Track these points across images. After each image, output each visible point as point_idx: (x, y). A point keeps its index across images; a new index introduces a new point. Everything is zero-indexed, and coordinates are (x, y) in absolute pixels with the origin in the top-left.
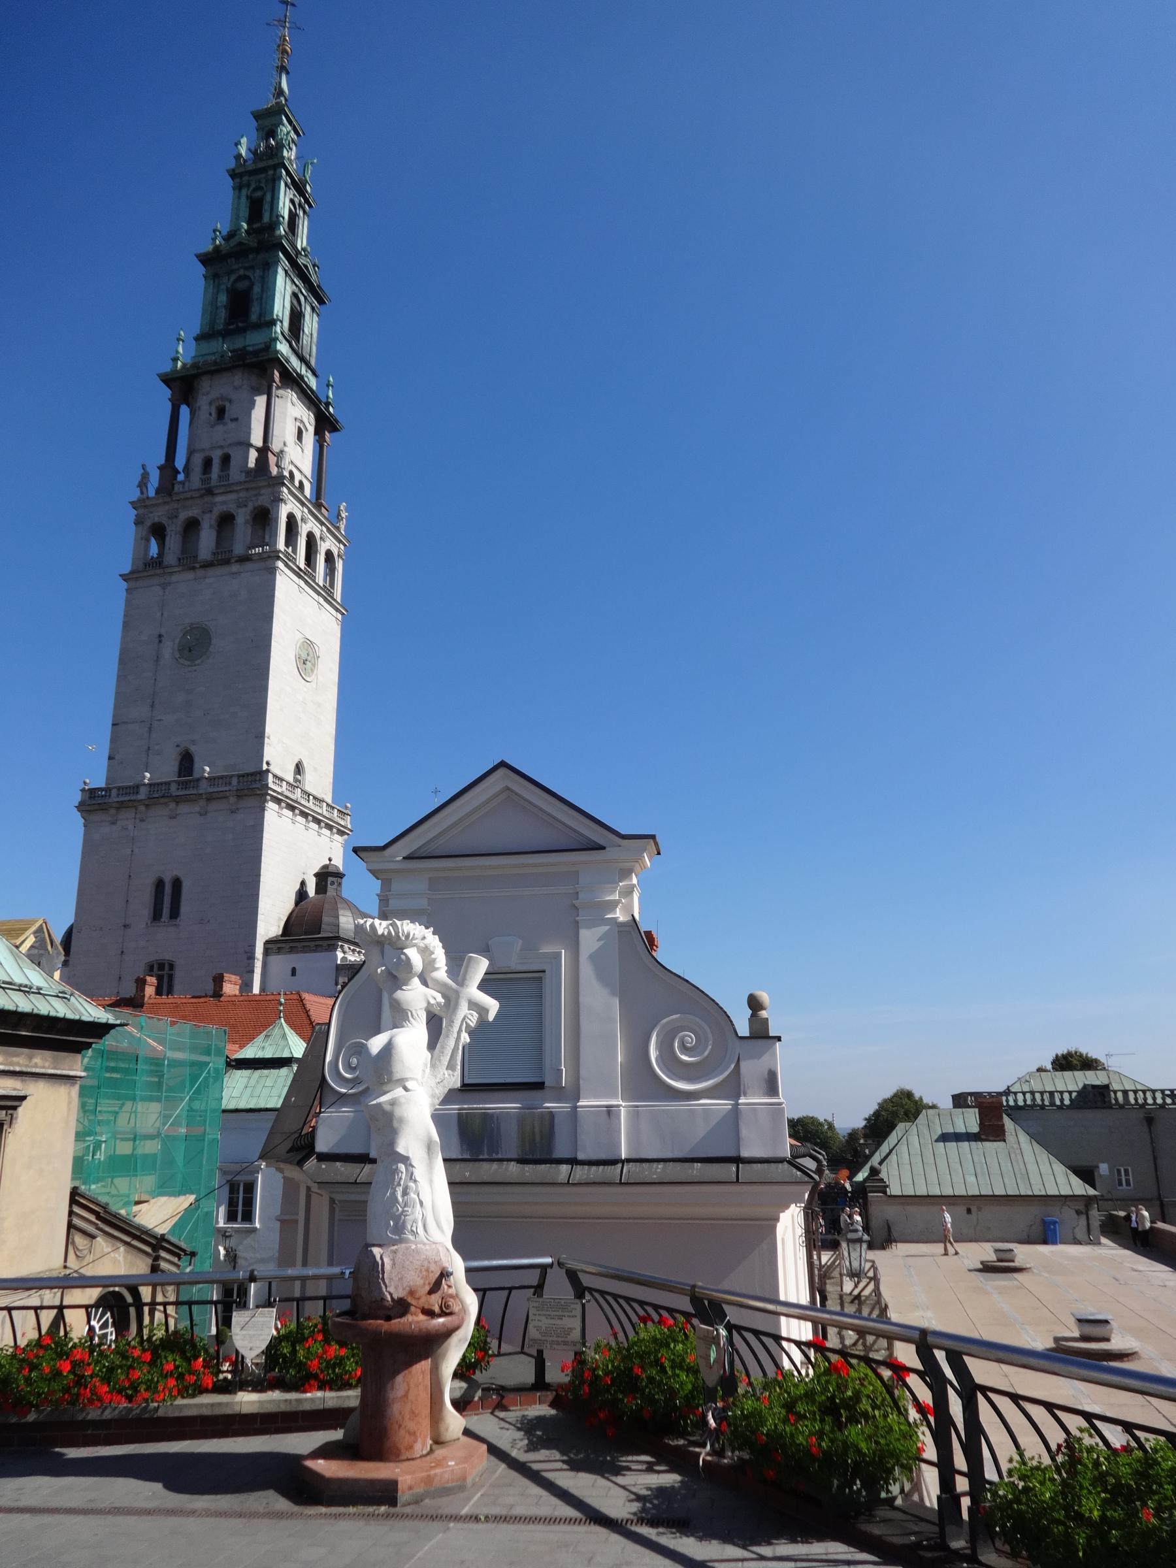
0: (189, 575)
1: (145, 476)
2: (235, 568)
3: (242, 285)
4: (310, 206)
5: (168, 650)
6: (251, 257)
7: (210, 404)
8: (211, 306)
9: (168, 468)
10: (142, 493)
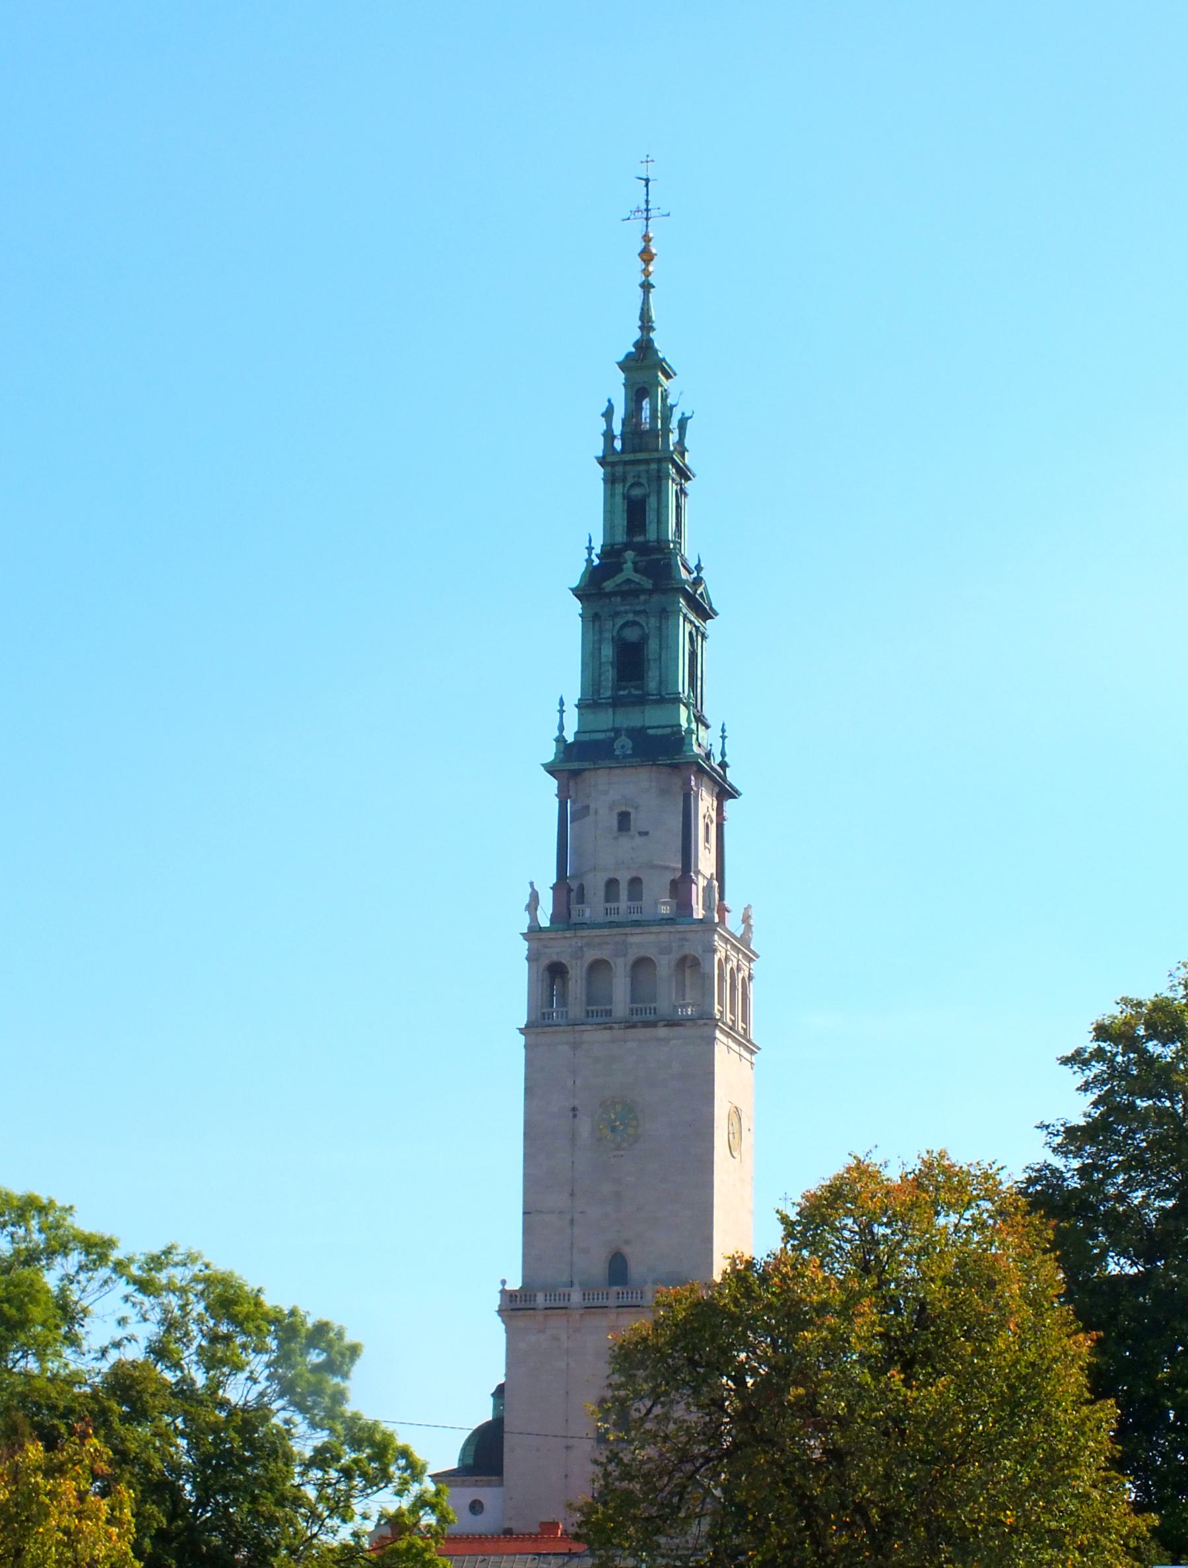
0: (606, 1035)
1: (534, 898)
2: (662, 1032)
3: (632, 635)
5: (585, 1128)
6: (642, 598)
7: (611, 809)
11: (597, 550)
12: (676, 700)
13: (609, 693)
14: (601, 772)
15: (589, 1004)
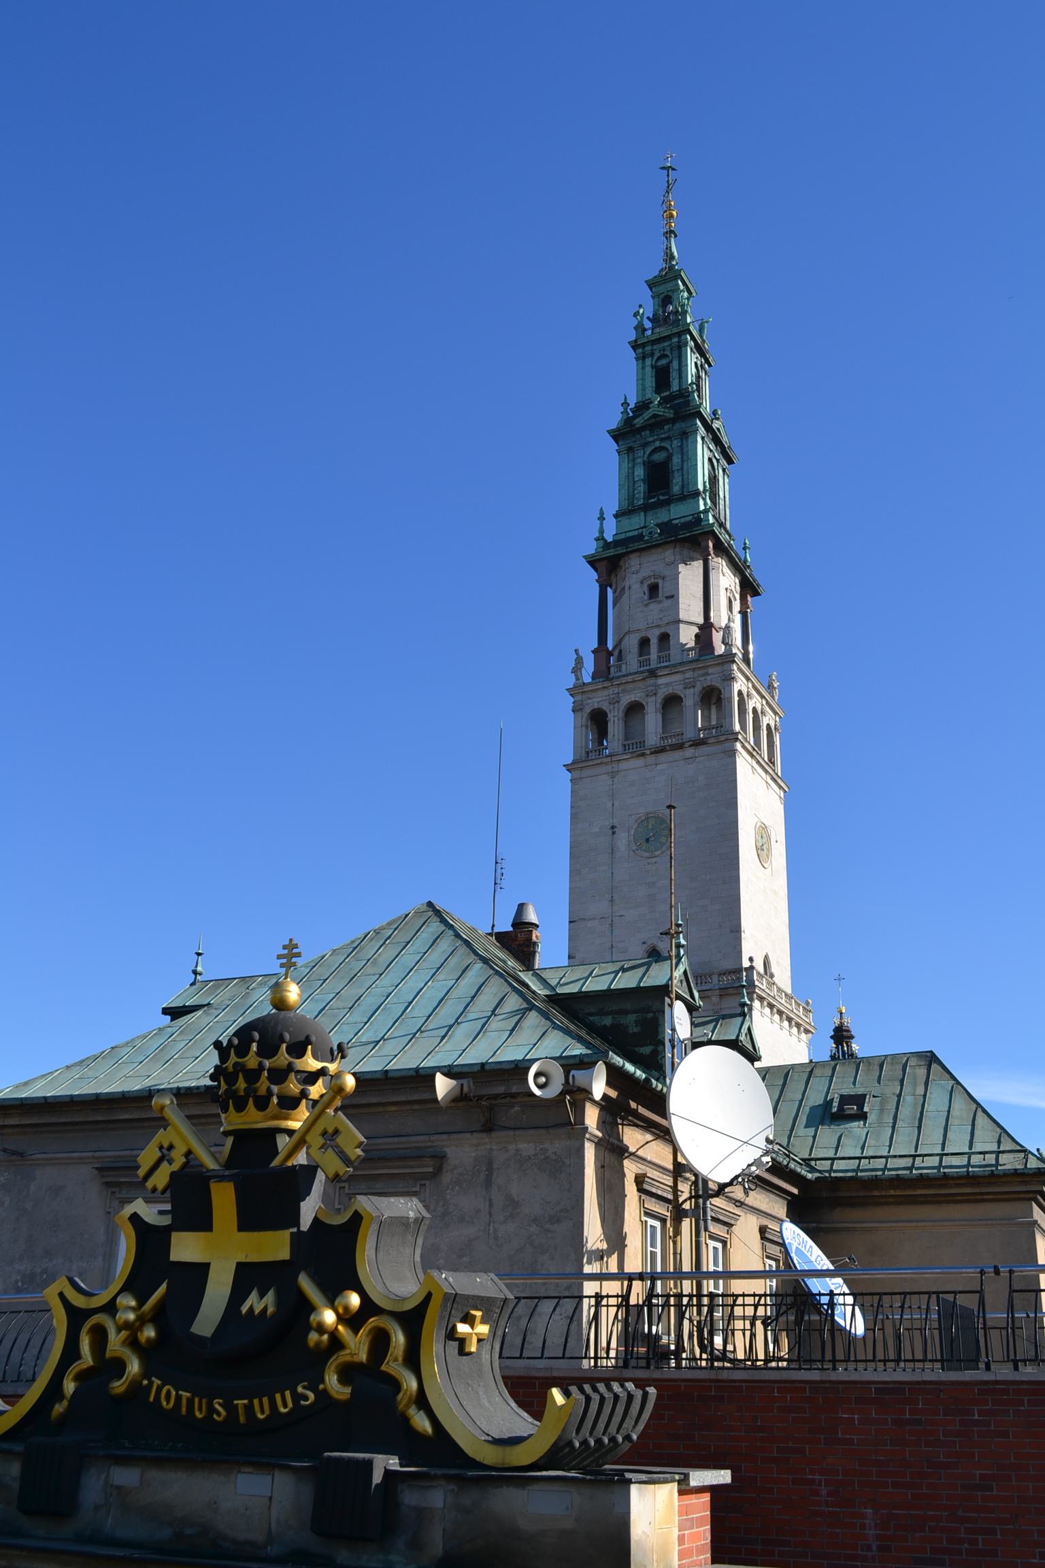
0: (640, 762)
2: (689, 752)
3: (660, 457)
4: (710, 365)
5: (623, 840)
7: (642, 583)
8: (628, 481)
9: (601, 651)
10: (577, 679)
11: (632, 406)
12: (696, 494)
13: (641, 502)
14: (632, 556)
15: (626, 739)
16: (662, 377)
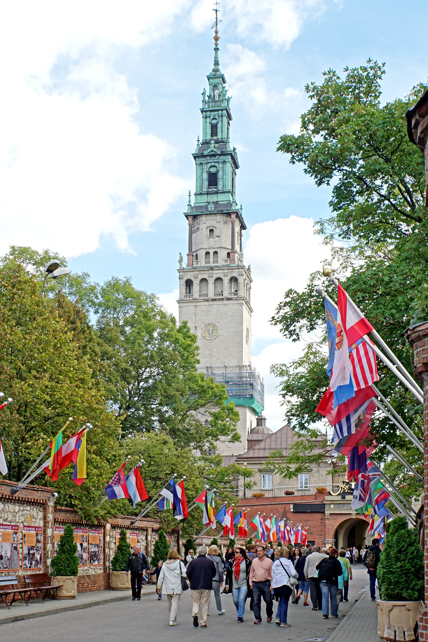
2: (226, 302)
3: (213, 170)
11: (201, 142)
16: (214, 129)
